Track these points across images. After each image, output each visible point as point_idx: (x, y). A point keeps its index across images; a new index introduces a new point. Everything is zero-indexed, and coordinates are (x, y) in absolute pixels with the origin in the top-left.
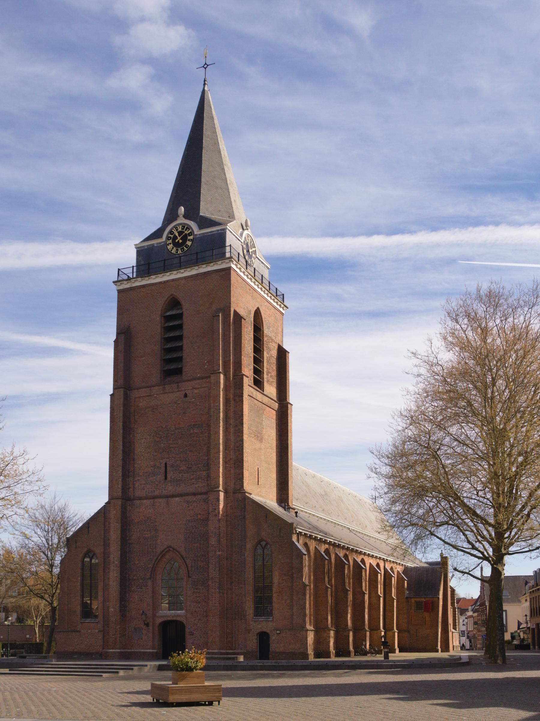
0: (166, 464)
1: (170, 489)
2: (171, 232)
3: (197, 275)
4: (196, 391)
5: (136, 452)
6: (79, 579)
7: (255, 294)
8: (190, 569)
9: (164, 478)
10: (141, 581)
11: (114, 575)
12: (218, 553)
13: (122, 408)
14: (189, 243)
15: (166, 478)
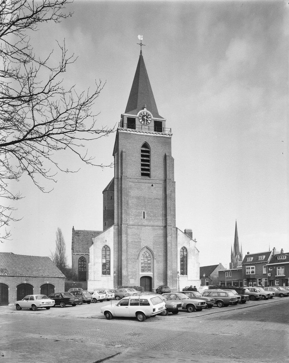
0: (144, 212)
2: (141, 114)
15: (144, 218)
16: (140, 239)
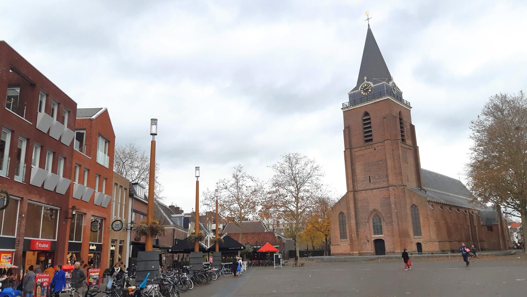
0: (369, 176)
1: (372, 186)
2: (362, 87)
3: (375, 103)
4: (379, 147)
5: (356, 172)
6: (338, 223)
8: (384, 218)
9: (369, 182)
10: (364, 223)
11: (353, 221)
12: (396, 211)
13: (350, 156)
15: (370, 182)
16: (368, 203)
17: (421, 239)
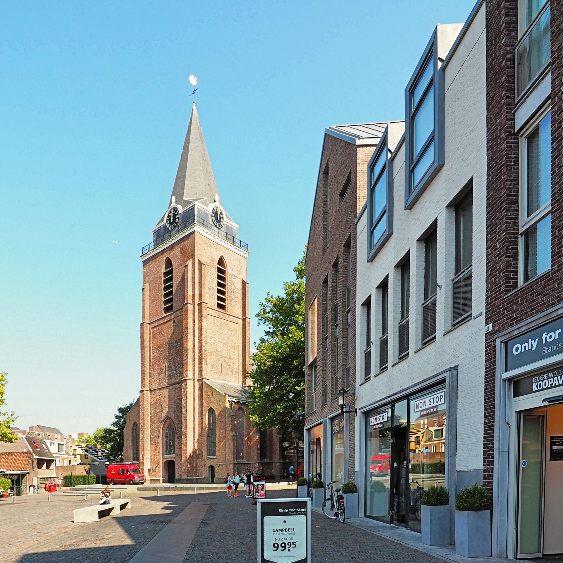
7: (219, 247)
14: (177, 220)
17: (215, 460)
